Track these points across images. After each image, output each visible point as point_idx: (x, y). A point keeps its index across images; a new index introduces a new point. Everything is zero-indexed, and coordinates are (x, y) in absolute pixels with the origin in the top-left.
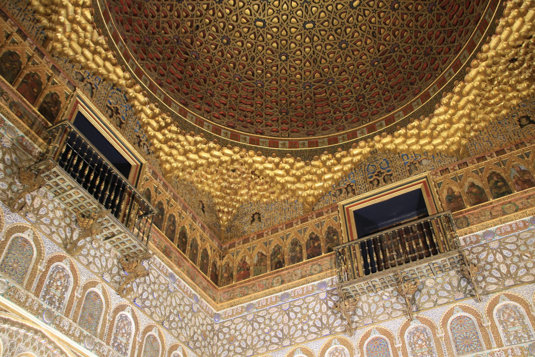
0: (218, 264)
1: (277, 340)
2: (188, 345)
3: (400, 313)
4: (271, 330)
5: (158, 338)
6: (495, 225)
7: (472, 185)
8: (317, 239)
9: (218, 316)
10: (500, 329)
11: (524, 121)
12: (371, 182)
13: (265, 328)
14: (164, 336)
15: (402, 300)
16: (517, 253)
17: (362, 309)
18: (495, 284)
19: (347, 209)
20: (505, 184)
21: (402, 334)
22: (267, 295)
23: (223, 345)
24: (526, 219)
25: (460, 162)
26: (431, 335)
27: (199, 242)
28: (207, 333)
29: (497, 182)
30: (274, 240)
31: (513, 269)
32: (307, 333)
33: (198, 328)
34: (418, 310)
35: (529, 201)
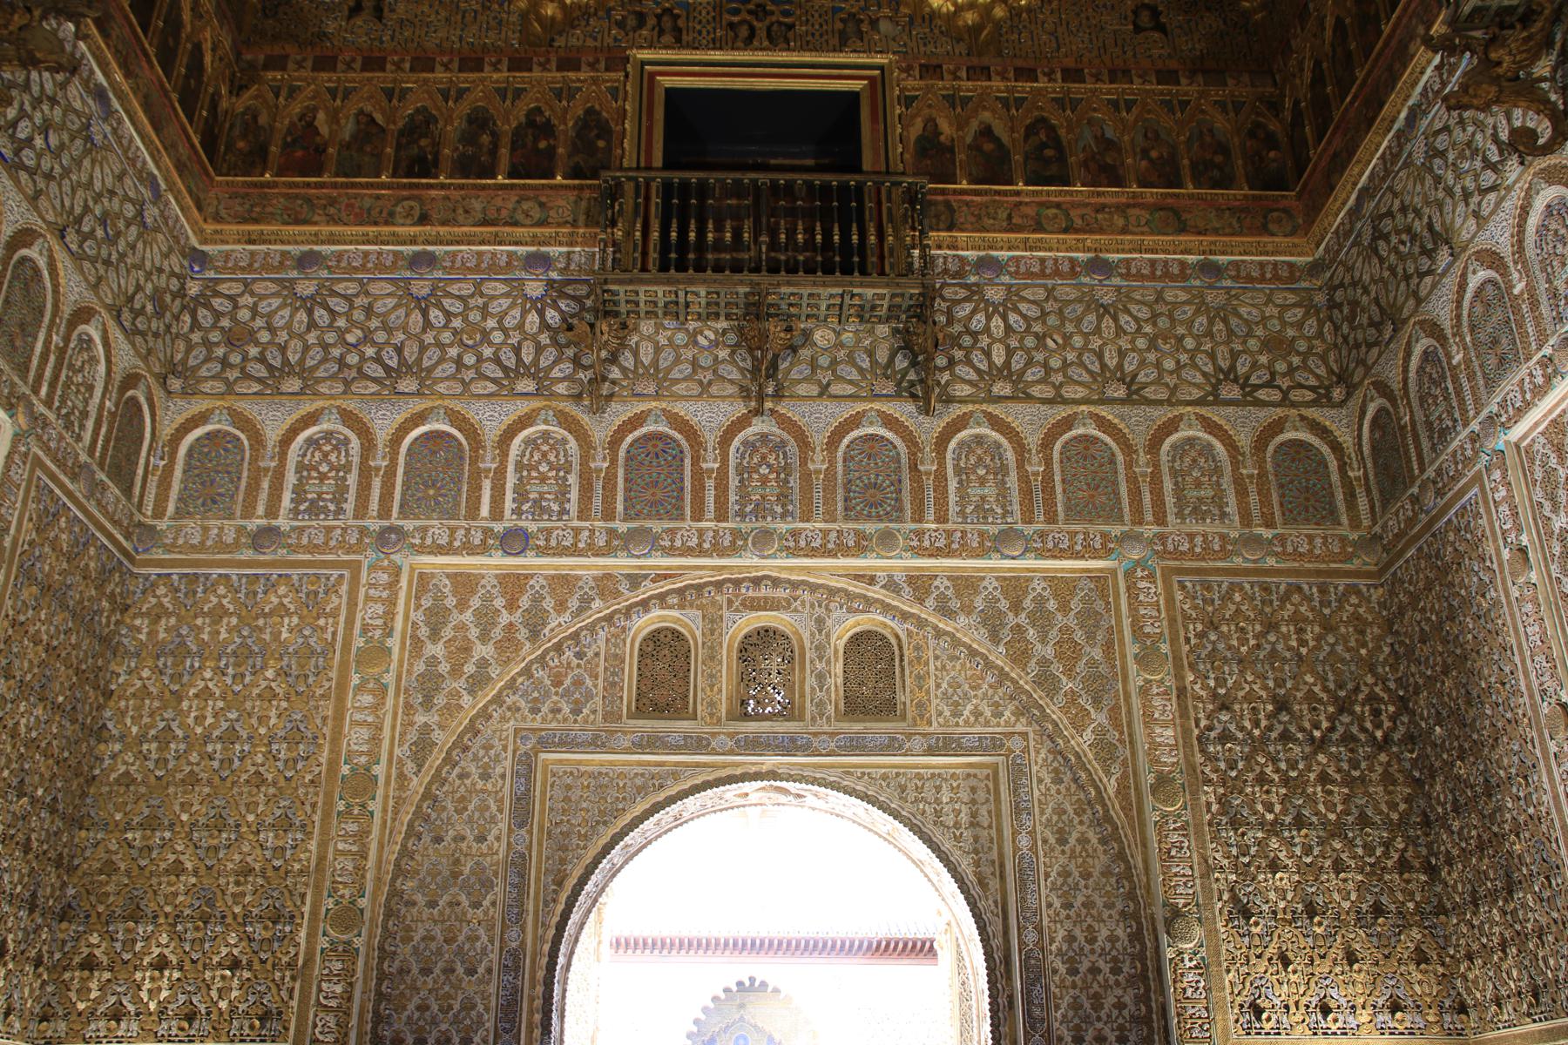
0: (224, 104)
1: (380, 373)
2: (118, 318)
3: (731, 390)
4: (367, 338)
5: (46, 273)
6: (1010, 249)
7: (987, 132)
8: (547, 130)
9: (201, 258)
10: (953, 484)
11: (1145, 18)
12: (731, 25)
13: (348, 331)
14: (62, 273)
15: (744, 360)
16: (1037, 328)
17: (636, 353)
18: (970, 382)
19: (652, 75)
20: (1061, 158)
21: (725, 441)
22: (369, 242)
23: (207, 344)
24: (1079, 255)
25: (975, 61)
26: (795, 461)
27: (186, 16)
28: (168, 298)
29: (1043, 146)
30: (419, 90)
31: (1017, 362)
32: (471, 374)
33: (148, 275)
34: (778, 395)
35: (1100, 216)
